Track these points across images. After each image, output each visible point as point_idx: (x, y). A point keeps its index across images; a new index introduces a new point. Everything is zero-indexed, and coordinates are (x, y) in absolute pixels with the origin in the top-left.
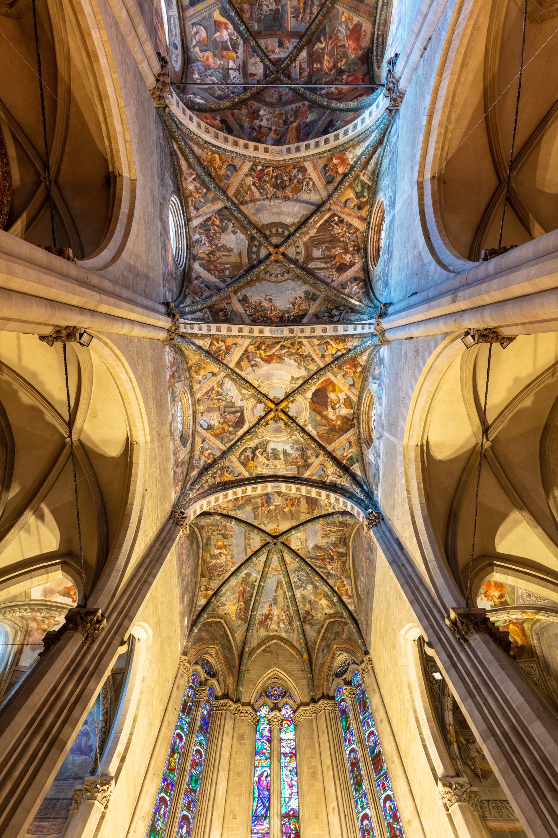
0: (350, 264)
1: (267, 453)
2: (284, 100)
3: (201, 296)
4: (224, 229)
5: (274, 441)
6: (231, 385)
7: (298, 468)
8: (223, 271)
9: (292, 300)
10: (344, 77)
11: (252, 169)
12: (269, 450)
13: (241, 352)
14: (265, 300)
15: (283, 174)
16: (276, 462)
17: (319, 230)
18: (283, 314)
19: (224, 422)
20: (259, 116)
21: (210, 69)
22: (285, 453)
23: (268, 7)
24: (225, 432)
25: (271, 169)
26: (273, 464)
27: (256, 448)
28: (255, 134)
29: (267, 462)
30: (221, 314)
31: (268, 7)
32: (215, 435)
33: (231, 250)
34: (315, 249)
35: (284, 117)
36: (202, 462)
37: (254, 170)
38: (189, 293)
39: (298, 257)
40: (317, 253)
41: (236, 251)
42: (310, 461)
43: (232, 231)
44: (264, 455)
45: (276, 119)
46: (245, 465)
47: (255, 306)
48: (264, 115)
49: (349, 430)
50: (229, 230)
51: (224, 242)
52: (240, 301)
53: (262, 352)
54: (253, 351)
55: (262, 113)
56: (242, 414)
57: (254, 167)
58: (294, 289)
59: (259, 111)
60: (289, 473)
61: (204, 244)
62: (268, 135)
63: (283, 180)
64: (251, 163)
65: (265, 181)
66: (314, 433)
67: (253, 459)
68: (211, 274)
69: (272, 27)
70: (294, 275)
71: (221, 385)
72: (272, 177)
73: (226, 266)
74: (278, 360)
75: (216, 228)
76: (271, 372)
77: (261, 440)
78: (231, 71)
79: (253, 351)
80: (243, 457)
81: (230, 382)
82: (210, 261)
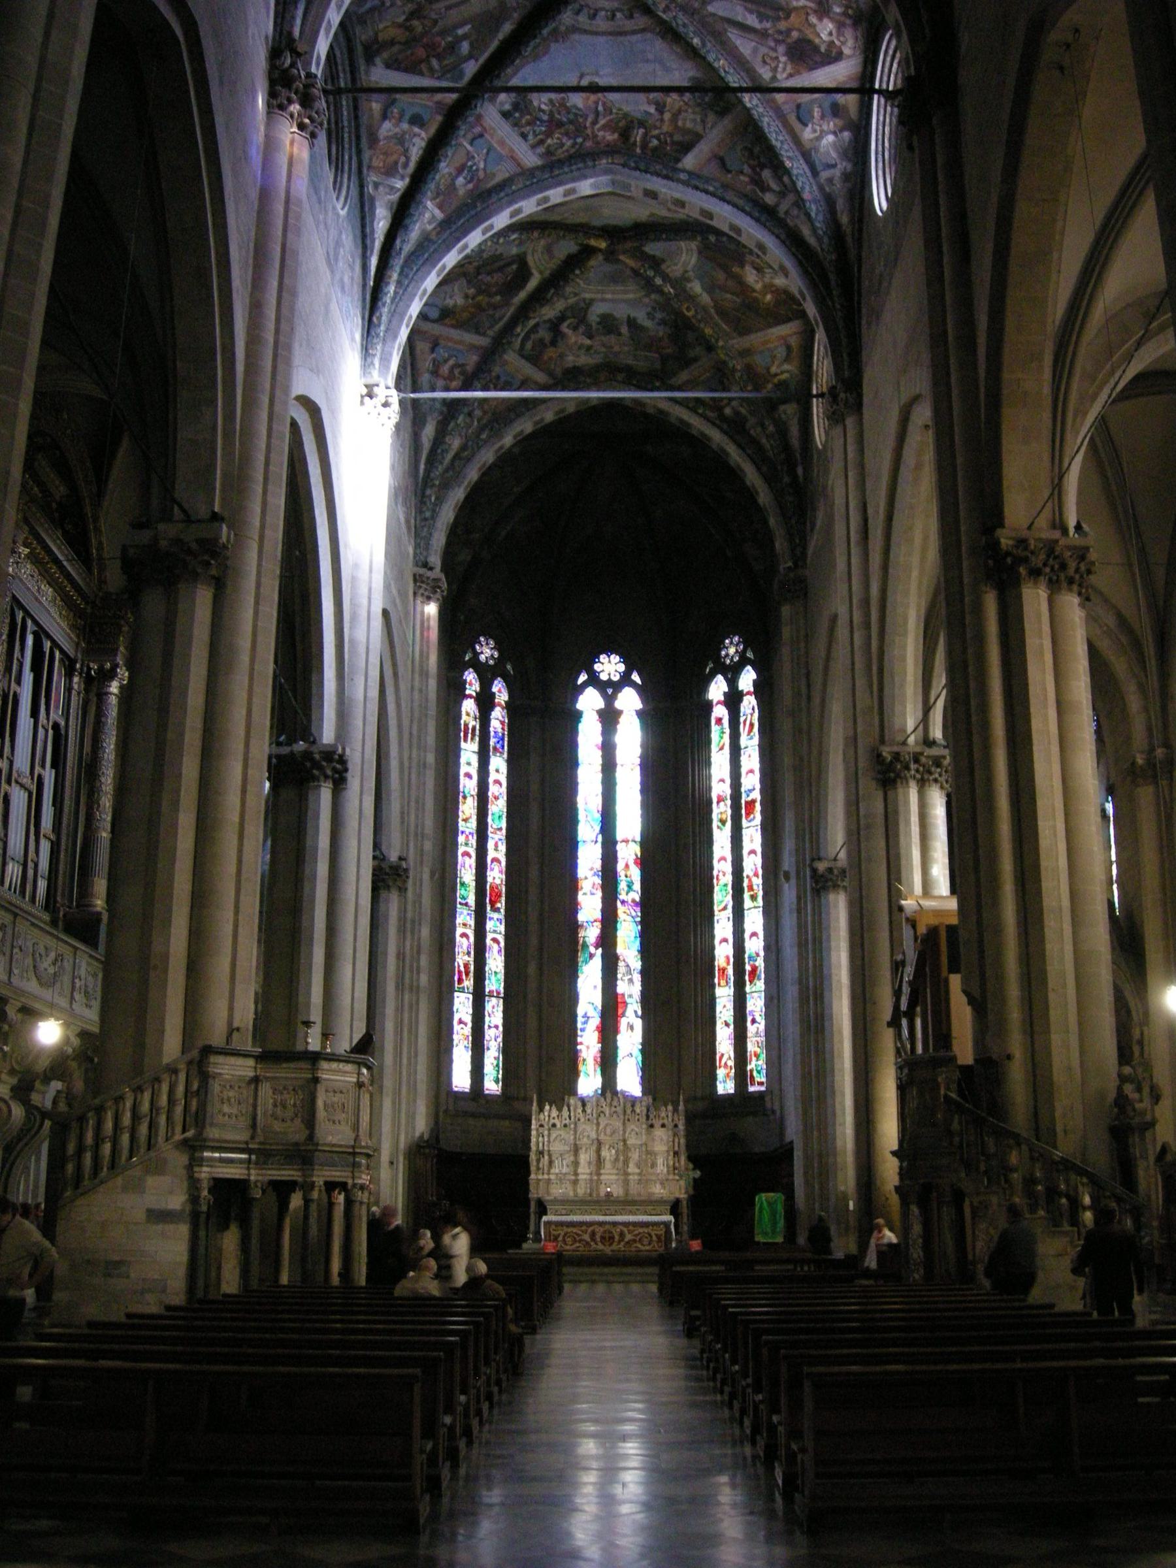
0: (828, 51)
1: (589, 326)
3: (406, 165)
5: (603, 300)
7: (664, 359)
8: (452, 48)
16: (613, 339)
22: (632, 323)
27: (562, 318)
30: (460, 181)
32: (459, 325)
38: (376, 185)
42: (692, 354)
44: (582, 329)
46: (534, 359)
47: (551, 114)
49: (789, 320)
52: (506, 115)
60: (641, 365)
66: (706, 299)
73: (460, 32)
77: (571, 301)
80: (529, 345)
82: (414, 39)
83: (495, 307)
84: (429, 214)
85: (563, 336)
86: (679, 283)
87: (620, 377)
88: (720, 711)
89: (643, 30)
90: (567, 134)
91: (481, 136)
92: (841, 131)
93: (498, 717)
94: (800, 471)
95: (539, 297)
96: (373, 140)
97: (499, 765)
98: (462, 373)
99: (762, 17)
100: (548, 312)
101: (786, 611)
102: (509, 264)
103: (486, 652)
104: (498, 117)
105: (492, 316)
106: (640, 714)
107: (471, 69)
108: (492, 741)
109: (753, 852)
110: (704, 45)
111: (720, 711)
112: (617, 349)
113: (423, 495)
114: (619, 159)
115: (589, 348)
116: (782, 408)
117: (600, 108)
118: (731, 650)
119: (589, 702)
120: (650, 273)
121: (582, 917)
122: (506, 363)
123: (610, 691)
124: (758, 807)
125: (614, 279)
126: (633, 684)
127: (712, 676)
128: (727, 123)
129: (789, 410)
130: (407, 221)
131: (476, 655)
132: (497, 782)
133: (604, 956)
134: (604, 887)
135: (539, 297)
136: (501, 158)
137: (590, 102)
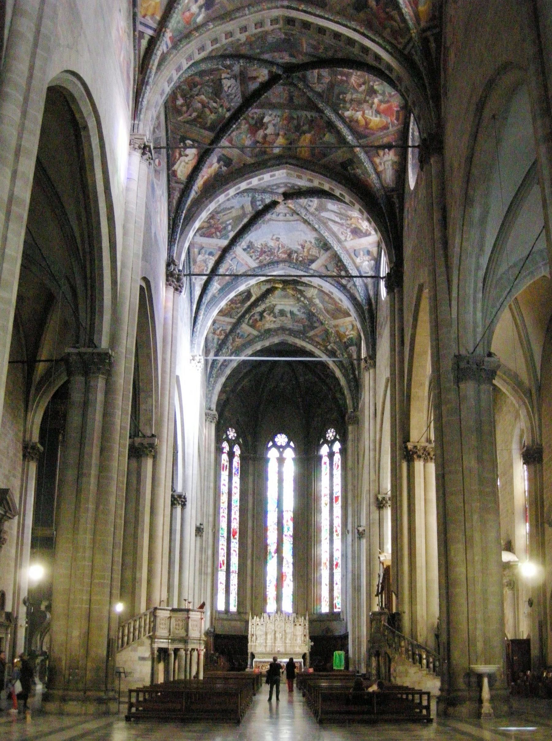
1: (274, 314)
7: (304, 326)
8: (225, 228)
9: (301, 242)
10: (376, 100)
12: (276, 310)
14: (272, 239)
16: (283, 318)
21: (195, 86)
22: (292, 313)
27: (264, 311)
33: (232, 207)
35: (295, 122)
36: (215, 341)
41: (238, 206)
44: (272, 315)
45: (285, 122)
46: (253, 326)
47: (262, 249)
48: (270, 122)
52: (244, 250)
55: (266, 120)
58: (304, 232)
59: (263, 117)
60: (296, 328)
66: (321, 305)
67: (261, 320)
68: (213, 237)
73: (228, 223)
77: (268, 305)
78: (224, 82)
80: (251, 321)
83: (238, 308)
84: (215, 286)
85: (265, 317)
86: (310, 300)
87: (287, 332)
88: (325, 459)
89: (297, 220)
90: (268, 255)
92: (371, 260)
93: (236, 461)
94: (357, 373)
95: (255, 304)
96: (195, 262)
97: (236, 480)
98: (225, 333)
99: (341, 219)
100: (259, 309)
101: (350, 428)
103: (232, 434)
106: (293, 459)
107: (232, 235)
108: (234, 471)
109: (338, 517)
110: (319, 227)
111: (325, 459)
112: (286, 322)
113: (209, 381)
114: (287, 264)
115: (275, 322)
116: (350, 348)
118: (331, 434)
119: (273, 454)
120: (299, 296)
121: (269, 541)
122: (242, 328)
123: (281, 450)
124: (340, 498)
125: (285, 297)
126: (291, 447)
127: (323, 443)
128: (328, 254)
129: (353, 349)
130: (207, 291)
131: (227, 436)
132: (236, 487)
133: (278, 557)
134: (278, 529)
135: (255, 304)
136: (242, 265)
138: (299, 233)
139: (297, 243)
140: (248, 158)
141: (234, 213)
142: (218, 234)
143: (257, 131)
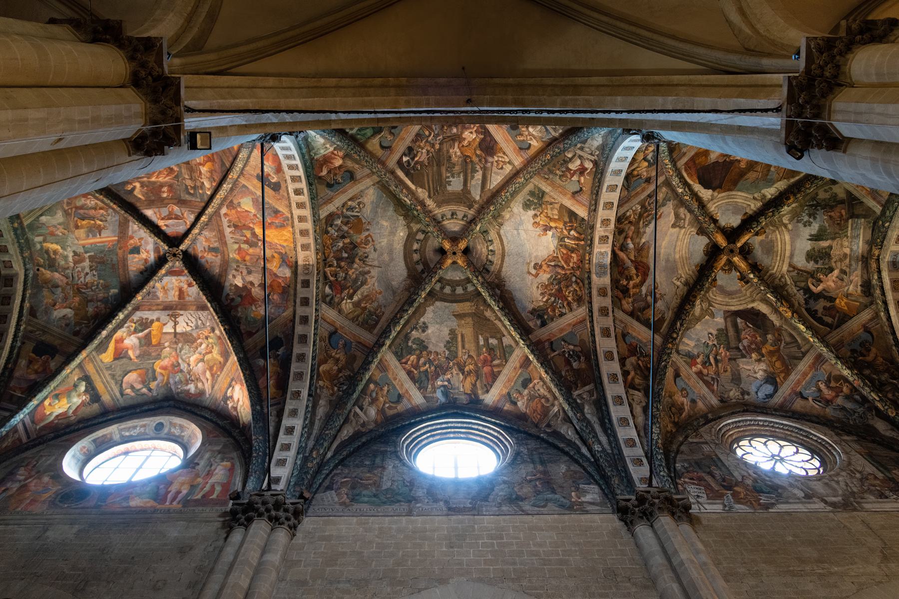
2: (216, 245)
4: (422, 346)
6: (690, 338)
8: (491, 350)
9: (539, 230)
11: (331, 304)
13: (636, 324)
14: (536, 276)
15: (335, 249)
17: (419, 183)
18: (566, 247)
19: (758, 350)
20: (245, 287)
23: (87, 274)
24: (778, 350)
25: (328, 270)
26: (841, 260)
28: (275, 297)
29: (836, 272)
31: (87, 274)
33: (452, 332)
34: (449, 188)
37: (332, 299)
39: (460, 215)
40: (455, 185)
43: (424, 331)
46: (845, 318)
48: (243, 279)
50: (423, 336)
51: (442, 345)
52: (544, 324)
53: (631, 283)
54: (630, 300)
55: (239, 282)
56: (737, 314)
57: (328, 299)
61: (449, 381)
62: (275, 275)
63: (342, 248)
64: (324, 306)
65: (345, 278)
67: (832, 299)
68: (499, 372)
69: (113, 265)
70: (490, 223)
71: (691, 358)
72: (339, 266)
73: (482, 343)
74: (644, 253)
75: (422, 360)
76: (664, 263)
79: (630, 300)
81: (685, 340)
83: (778, 340)
90: (567, 287)
91: (552, 343)
102: (735, 325)
104: (543, 329)
105: (787, 344)
117: (553, 264)
137: (548, 270)
138: (522, 232)
139: (544, 238)
140: (284, 314)
141: (468, 331)
142: (496, 362)
143: (252, 297)
